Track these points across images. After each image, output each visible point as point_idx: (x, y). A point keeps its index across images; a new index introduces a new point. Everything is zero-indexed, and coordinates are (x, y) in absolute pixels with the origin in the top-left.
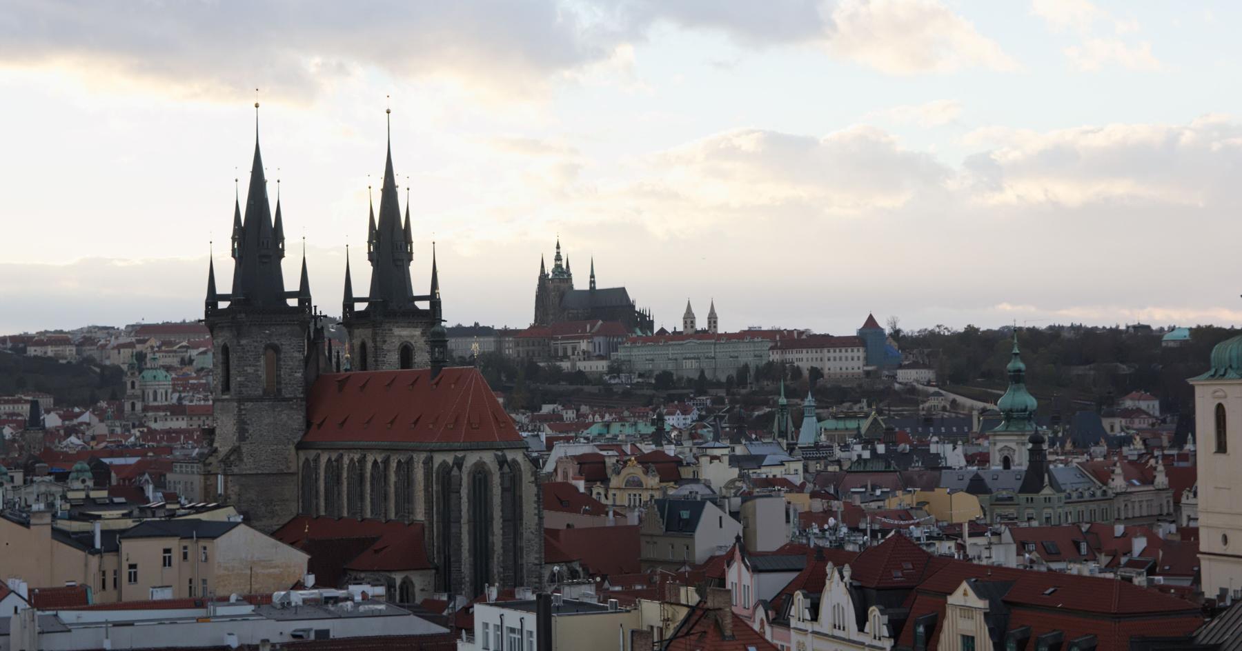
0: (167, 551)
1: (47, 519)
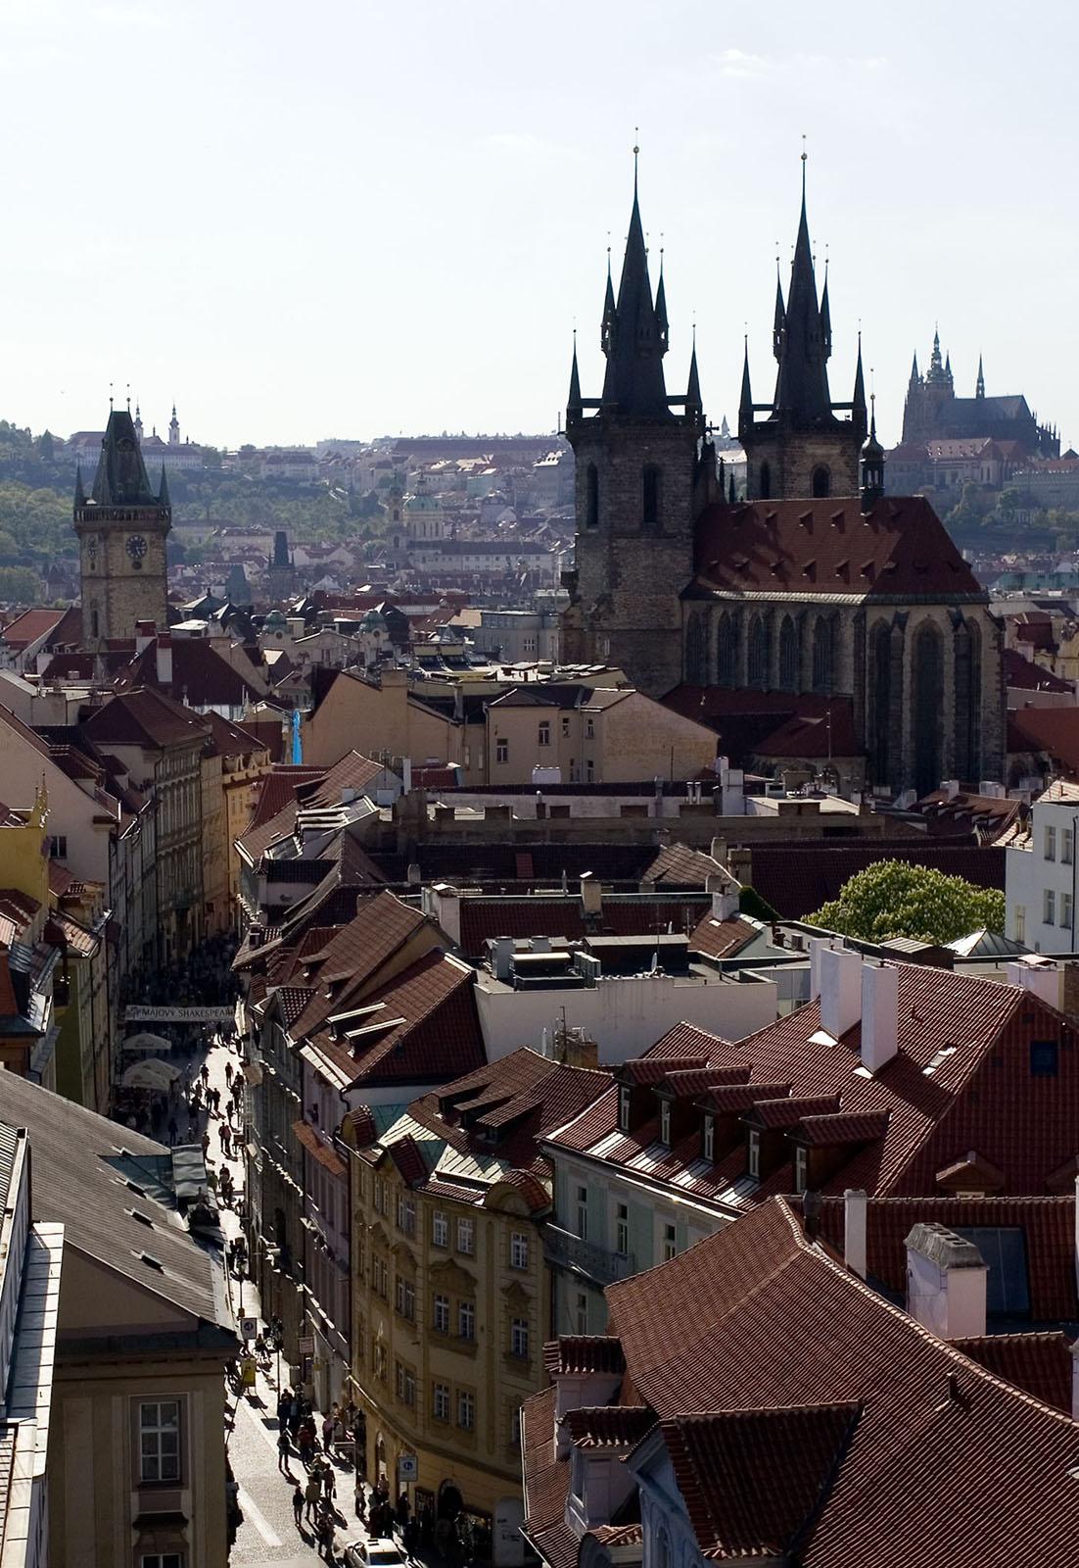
0: (545, 724)
1: (403, 680)
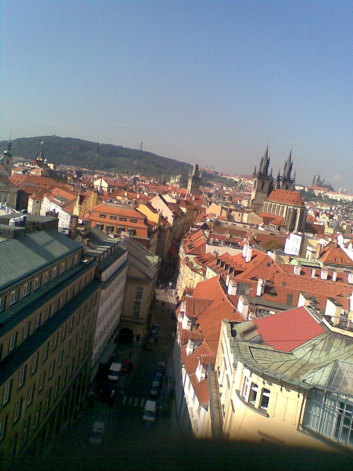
1: (221, 204)
